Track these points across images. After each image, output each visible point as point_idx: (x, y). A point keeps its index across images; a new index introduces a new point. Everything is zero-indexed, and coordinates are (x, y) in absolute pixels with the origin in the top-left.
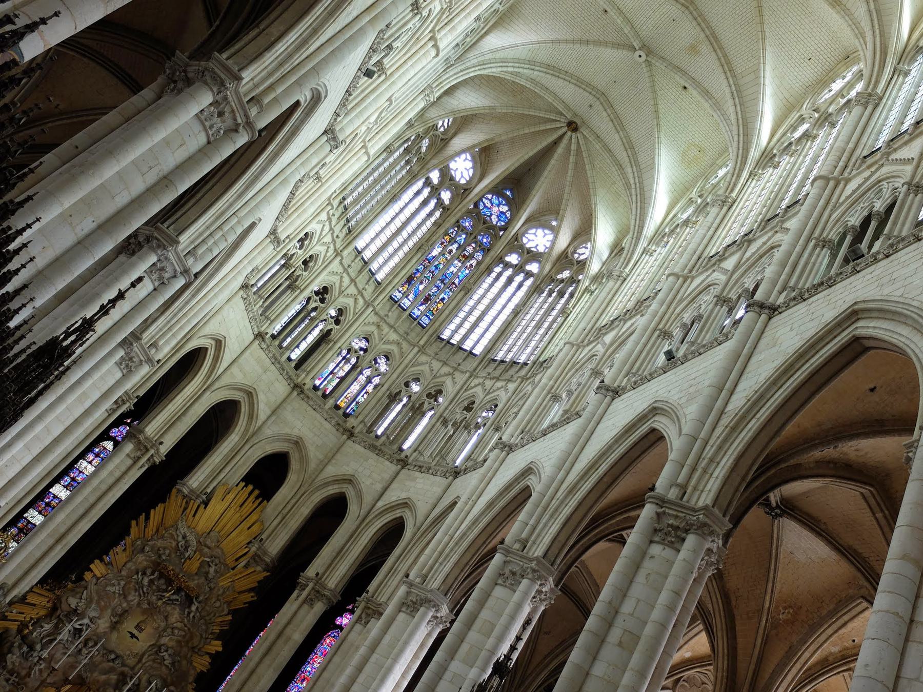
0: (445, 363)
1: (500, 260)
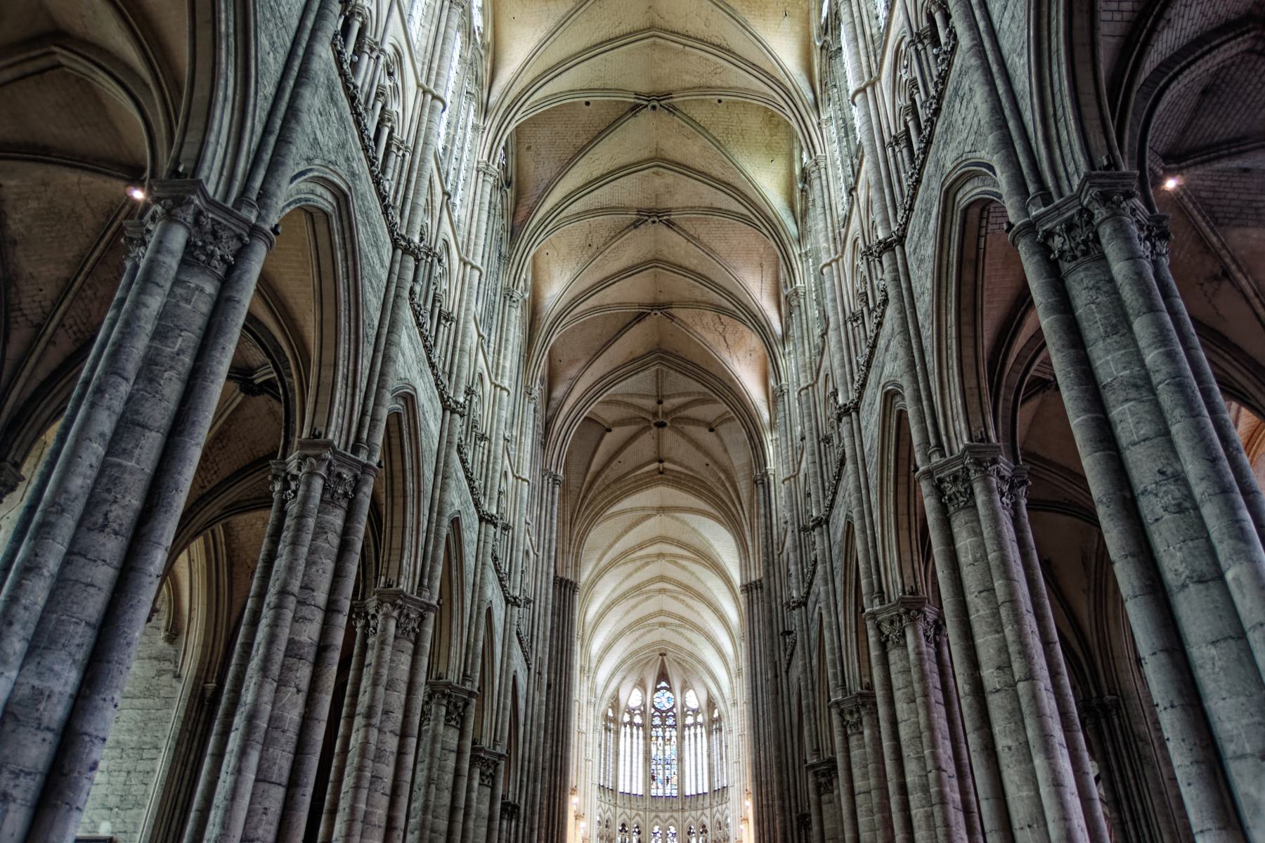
0: (696, 810)
1: (684, 726)
